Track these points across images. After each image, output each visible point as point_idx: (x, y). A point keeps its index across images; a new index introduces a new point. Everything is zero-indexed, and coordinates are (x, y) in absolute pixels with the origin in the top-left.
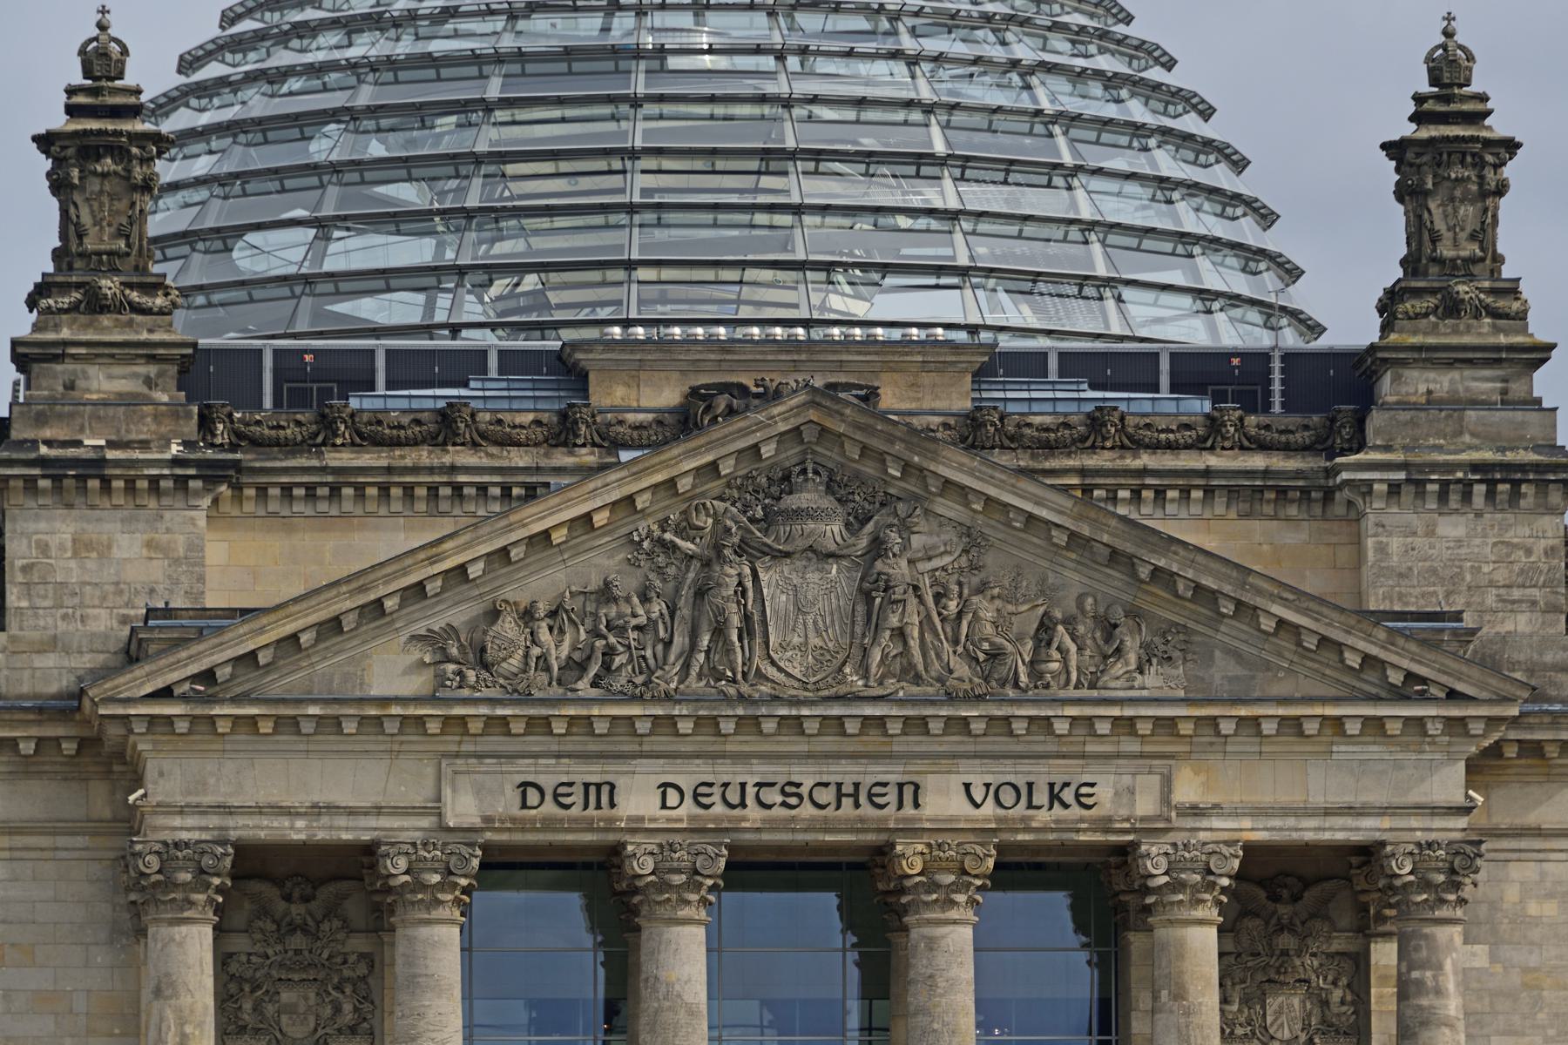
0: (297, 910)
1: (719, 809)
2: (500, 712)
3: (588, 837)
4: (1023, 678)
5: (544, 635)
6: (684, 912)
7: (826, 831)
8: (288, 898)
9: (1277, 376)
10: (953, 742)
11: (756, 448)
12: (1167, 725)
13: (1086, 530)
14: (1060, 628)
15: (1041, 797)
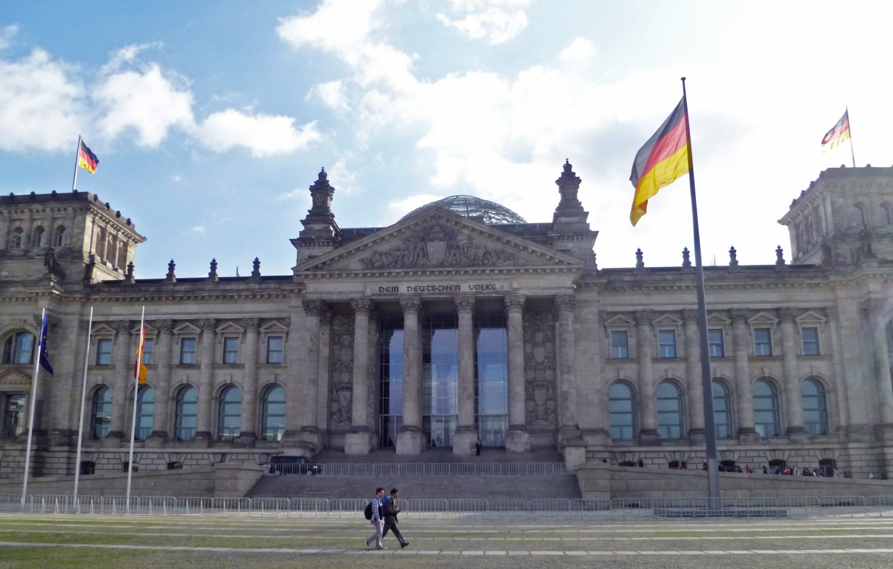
0: (346, 321)
1: (419, 291)
2: (374, 271)
3: (392, 297)
4: (480, 263)
5: (384, 258)
6: (411, 312)
7: (440, 294)
8: (344, 318)
9: (538, 228)
10: (466, 277)
11: (426, 220)
12: (509, 271)
13: (492, 233)
14: (487, 254)
15: (485, 287)
